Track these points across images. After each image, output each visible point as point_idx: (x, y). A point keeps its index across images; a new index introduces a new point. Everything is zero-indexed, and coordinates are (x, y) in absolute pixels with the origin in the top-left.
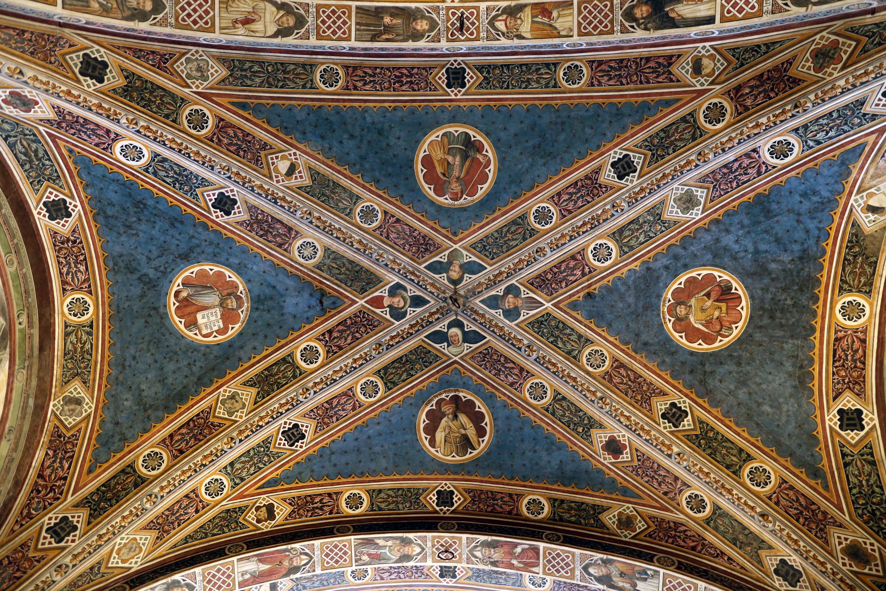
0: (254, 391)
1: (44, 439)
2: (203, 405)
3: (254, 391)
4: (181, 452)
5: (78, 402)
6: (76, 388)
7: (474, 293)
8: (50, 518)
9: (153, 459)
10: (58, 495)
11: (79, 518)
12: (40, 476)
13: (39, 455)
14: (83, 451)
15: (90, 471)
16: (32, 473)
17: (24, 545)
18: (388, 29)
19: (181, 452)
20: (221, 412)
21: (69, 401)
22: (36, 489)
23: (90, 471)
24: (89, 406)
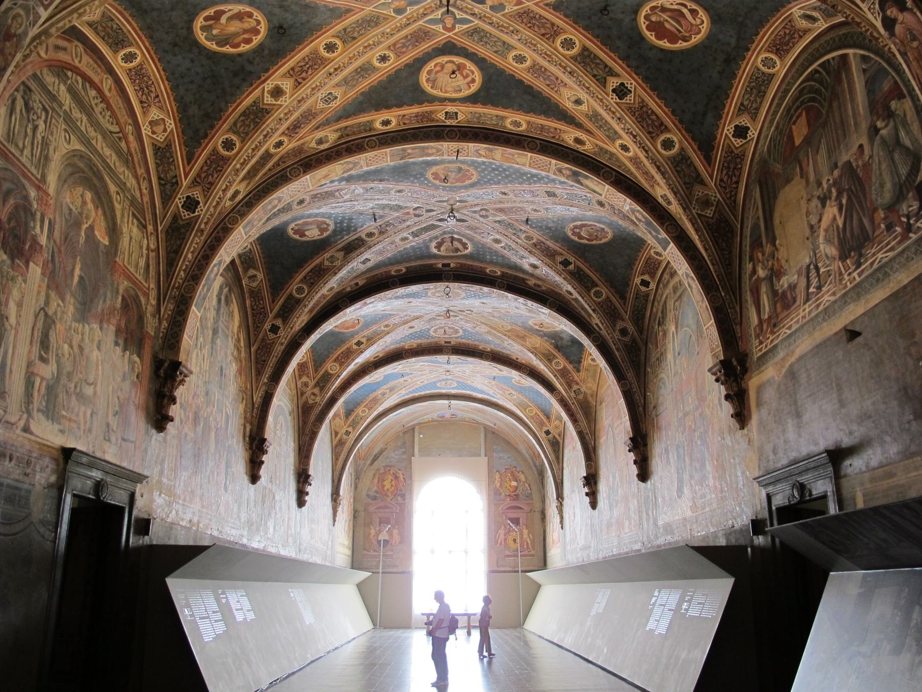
0: (342, 253)
1: (247, 295)
2: (317, 261)
3: (342, 253)
4: (312, 284)
5: (255, 276)
6: (252, 272)
7: (463, 208)
8: (267, 326)
9: (300, 290)
10: (266, 316)
11: (279, 322)
12: (253, 310)
13: (248, 302)
14: (266, 294)
15: (273, 302)
16: (249, 310)
17: (263, 340)
18: (409, 154)
19: (312, 284)
20: (327, 263)
21: (250, 278)
22: (253, 315)
23: (273, 302)
24: (260, 276)
